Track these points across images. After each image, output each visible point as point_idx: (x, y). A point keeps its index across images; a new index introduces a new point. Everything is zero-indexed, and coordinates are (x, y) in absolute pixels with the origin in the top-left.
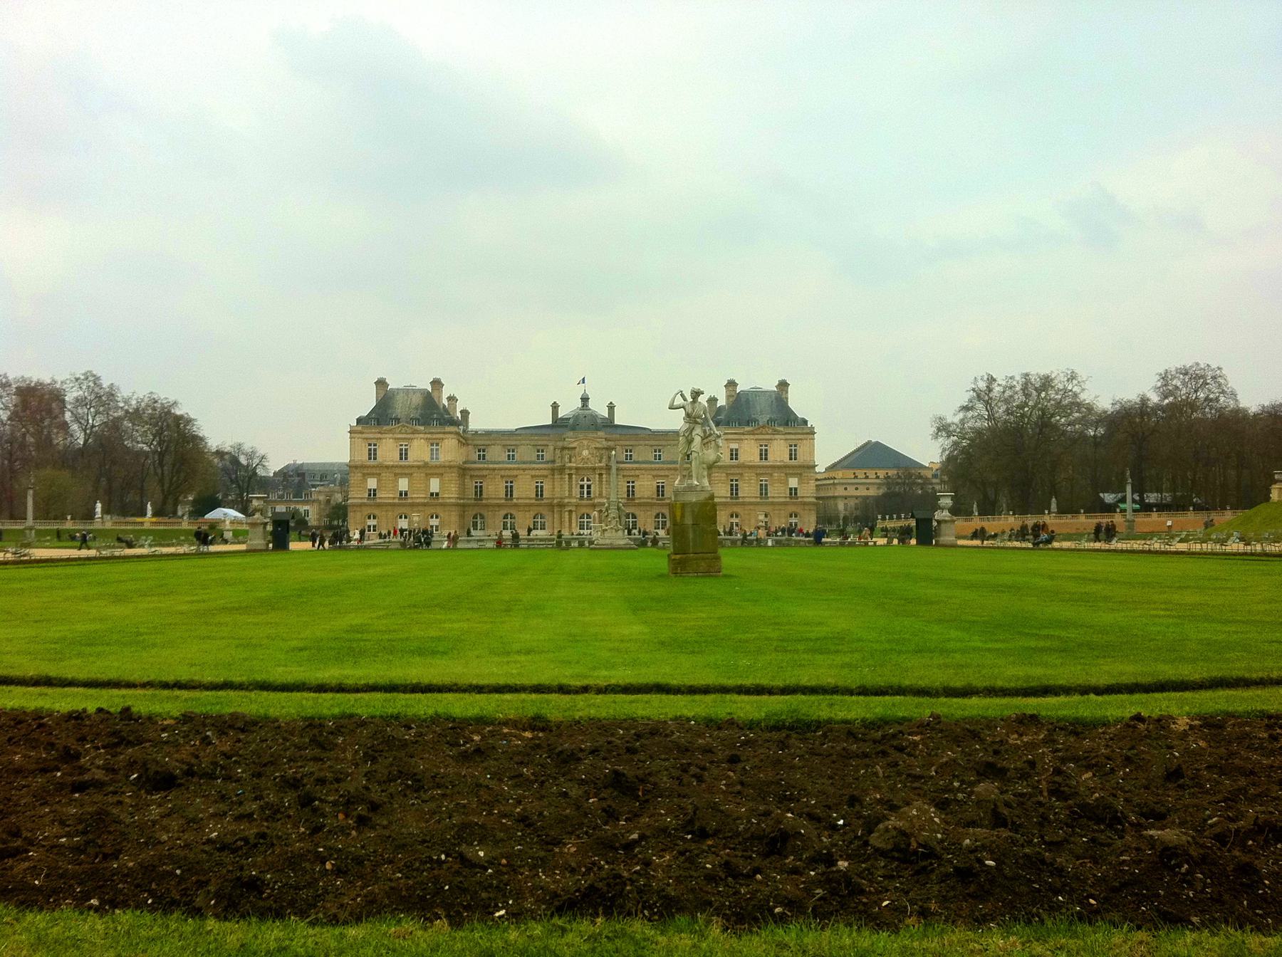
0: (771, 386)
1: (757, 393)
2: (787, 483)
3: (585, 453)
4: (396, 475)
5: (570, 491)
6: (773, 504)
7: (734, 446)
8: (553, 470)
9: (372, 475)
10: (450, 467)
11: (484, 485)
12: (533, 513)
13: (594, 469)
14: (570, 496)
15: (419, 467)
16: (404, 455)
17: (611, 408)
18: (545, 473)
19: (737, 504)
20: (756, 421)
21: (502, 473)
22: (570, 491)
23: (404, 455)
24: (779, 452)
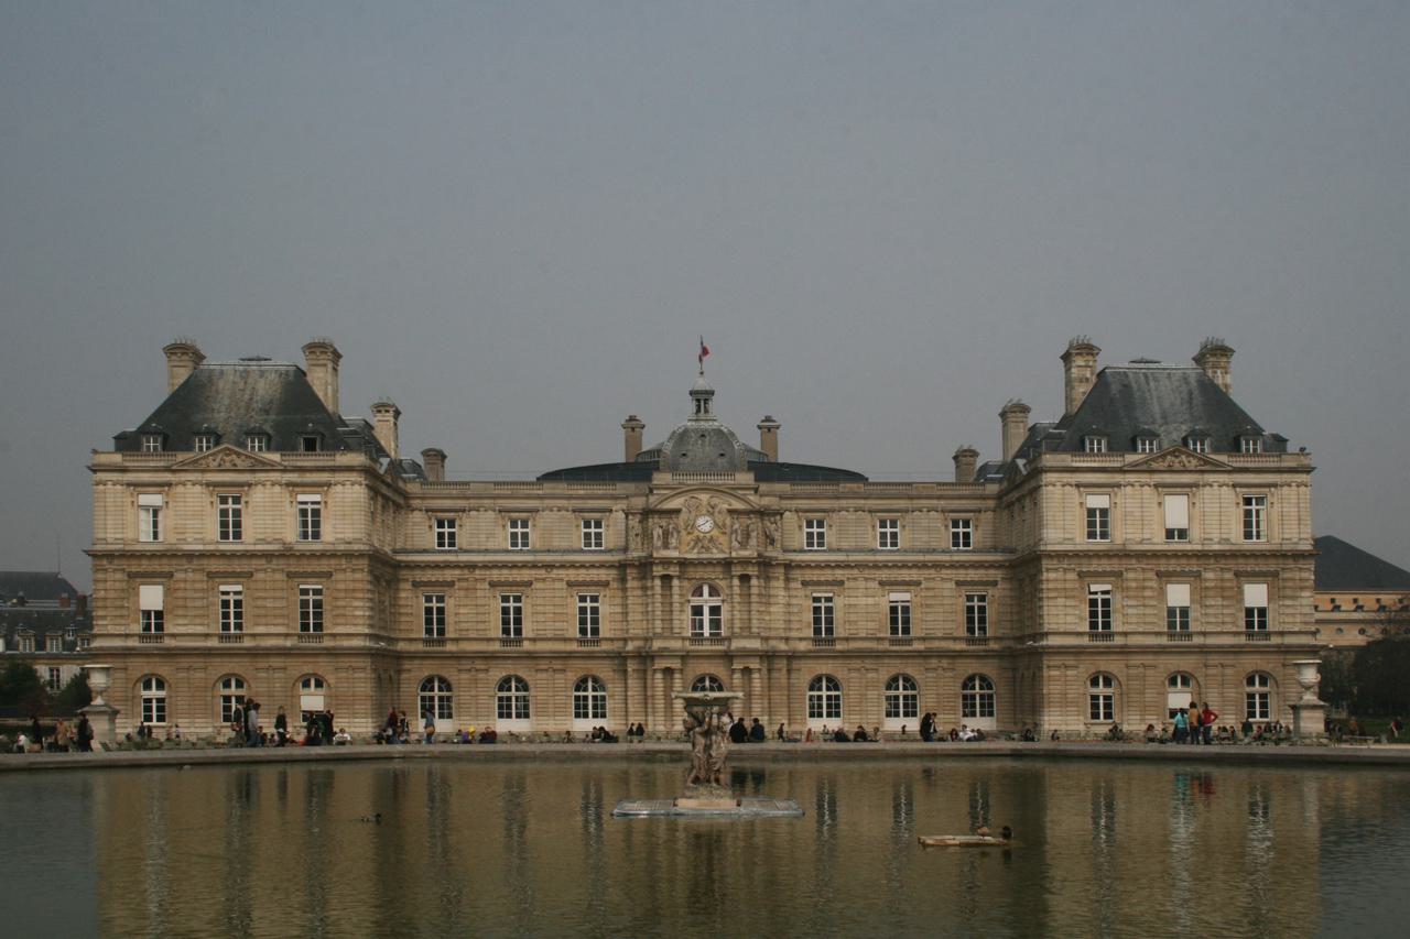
2: (1239, 595)
3: (705, 525)
4: (211, 575)
6: (1203, 650)
7: (1098, 501)
8: (622, 567)
9: (150, 577)
10: (349, 555)
11: (449, 604)
12: (573, 677)
13: (727, 564)
15: (268, 556)
16: (231, 526)
17: (768, 427)
18: (603, 575)
19: (1108, 651)
20: (1152, 435)
22: (668, 620)
23: (231, 526)
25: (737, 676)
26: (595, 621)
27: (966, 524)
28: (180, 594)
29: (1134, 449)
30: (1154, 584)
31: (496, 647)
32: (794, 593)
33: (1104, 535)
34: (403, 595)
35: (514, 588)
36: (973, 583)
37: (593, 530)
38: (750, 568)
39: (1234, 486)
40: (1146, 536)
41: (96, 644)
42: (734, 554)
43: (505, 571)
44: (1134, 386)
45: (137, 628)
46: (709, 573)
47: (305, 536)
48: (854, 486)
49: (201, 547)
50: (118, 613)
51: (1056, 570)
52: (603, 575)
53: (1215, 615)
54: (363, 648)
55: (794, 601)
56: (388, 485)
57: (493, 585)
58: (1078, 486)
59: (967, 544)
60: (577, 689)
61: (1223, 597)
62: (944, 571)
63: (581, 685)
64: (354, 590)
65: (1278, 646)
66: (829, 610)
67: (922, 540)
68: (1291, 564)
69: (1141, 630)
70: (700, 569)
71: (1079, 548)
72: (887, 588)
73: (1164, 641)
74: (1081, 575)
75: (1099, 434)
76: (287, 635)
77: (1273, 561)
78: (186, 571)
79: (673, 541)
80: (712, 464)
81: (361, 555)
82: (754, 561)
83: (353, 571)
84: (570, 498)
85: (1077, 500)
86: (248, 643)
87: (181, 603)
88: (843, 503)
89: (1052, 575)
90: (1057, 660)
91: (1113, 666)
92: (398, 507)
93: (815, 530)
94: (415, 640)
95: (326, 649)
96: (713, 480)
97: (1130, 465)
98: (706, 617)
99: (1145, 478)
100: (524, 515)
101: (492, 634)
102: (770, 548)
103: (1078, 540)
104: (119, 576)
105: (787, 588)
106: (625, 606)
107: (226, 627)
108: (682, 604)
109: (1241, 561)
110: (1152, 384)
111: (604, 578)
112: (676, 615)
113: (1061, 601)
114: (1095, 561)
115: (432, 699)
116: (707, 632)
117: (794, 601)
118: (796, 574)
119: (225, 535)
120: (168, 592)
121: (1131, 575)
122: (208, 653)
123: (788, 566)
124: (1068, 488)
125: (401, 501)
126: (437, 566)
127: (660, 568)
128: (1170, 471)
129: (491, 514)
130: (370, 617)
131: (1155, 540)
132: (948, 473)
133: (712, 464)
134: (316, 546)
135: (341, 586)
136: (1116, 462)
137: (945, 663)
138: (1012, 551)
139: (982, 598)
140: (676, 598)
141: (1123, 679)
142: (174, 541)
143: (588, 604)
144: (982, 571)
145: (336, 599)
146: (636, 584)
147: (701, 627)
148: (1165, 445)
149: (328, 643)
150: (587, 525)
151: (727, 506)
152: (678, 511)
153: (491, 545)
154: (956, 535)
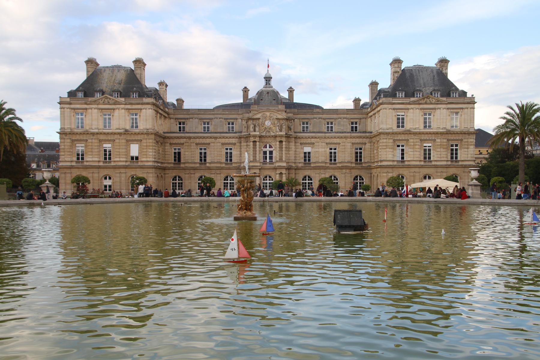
0: (431, 62)
1: (420, 69)
3: (268, 123)
4: (100, 141)
5: (255, 156)
6: (436, 167)
8: (240, 138)
10: (147, 134)
11: (182, 151)
12: (223, 176)
13: (276, 137)
15: (120, 134)
17: (291, 91)
18: (233, 141)
19: (403, 167)
21: (198, 141)
22: (255, 156)
23: (107, 123)
24: (442, 118)
25: (278, 175)
26: (231, 157)
27: (356, 123)
28: (90, 147)
29: (414, 97)
31: (198, 165)
32: (297, 147)
33: (403, 127)
34: (166, 148)
36: (357, 143)
37: (231, 126)
38: (283, 138)
39: (448, 109)
41: (61, 164)
42: (277, 134)
43: (201, 140)
44: (415, 74)
45: (75, 159)
46: (269, 140)
47: (132, 127)
48: (318, 110)
49: (97, 131)
50: (69, 153)
51: (386, 139)
52: (233, 141)
53: (440, 155)
54: (152, 165)
55: (297, 150)
56: (162, 110)
57: (197, 144)
59: (356, 130)
60: (225, 180)
61: (444, 148)
62: (348, 139)
63: (226, 179)
64: (149, 146)
65: (462, 165)
67: (341, 128)
68: (467, 136)
70: (266, 138)
71: (394, 131)
73: (422, 163)
74: (394, 141)
75: (402, 91)
76: (126, 161)
77: (461, 135)
78: (92, 139)
79: (257, 129)
80: (271, 102)
81: (152, 134)
83: (149, 139)
84: (223, 114)
85: (394, 114)
86: (112, 164)
87: (90, 150)
88: (315, 116)
89: (385, 141)
90: (385, 170)
92: (165, 117)
93: (305, 126)
94: (171, 163)
95: (139, 166)
96: (271, 108)
97: (412, 101)
98: (268, 155)
99: (417, 106)
100: (208, 120)
101: (196, 161)
102: (290, 131)
103: (394, 128)
104: (69, 141)
105: (295, 146)
106: (240, 151)
107: (105, 159)
108: (260, 151)
109: (450, 135)
110: (421, 73)
111: (234, 142)
112: (257, 155)
113: (388, 150)
114: (399, 136)
115: (176, 183)
116: (268, 160)
117: (297, 150)
118: (299, 141)
119: (105, 126)
120: (86, 146)
121: (412, 140)
122: (99, 167)
123: (296, 138)
125: (166, 115)
126: (178, 138)
127: (252, 138)
128: (426, 103)
129: (197, 120)
130: (155, 155)
132: (350, 105)
133: (271, 102)
134: (137, 131)
135: (145, 144)
136: (407, 100)
137: (348, 171)
138: (371, 132)
139: (361, 149)
140: (258, 149)
141: (408, 177)
142: (88, 128)
143: (229, 151)
144: (361, 139)
145: (143, 149)
146: (245, 144)
147: (266, 159)
148: (425, 94)
149: (140, 164)
150: (229, 124)
151: (275, 117)
152: (259, 119)
153: (197, 131)
154: (352, 127)
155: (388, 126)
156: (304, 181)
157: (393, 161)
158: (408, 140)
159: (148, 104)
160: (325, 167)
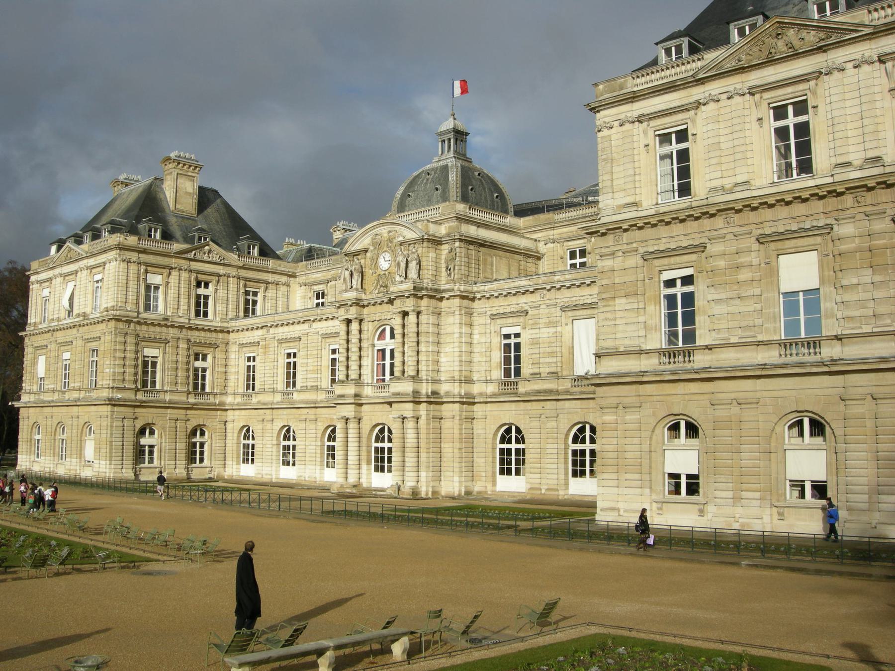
3: (384, 263)
6: (835, 369)
14: (347, 376)
30: (754, 258)
35: (292, 344)
40: (740, 179)
43: (286, 329)
53: (861, 304)
57: (281, 341)
58: (640, 120)
66: (518, 346)
69: (734, 340)
72: (570, 314)
74: (647, 257)
79: (354, 282)
82: (406, 294)
91: (691, 401)
124: (628, 126)
128: (771, 61)
131: (757, 183)
147: (384, 375)
152: (366, 251)
155: (622, 199)
156: (506, 446)
157: (641, 352)
158: (702, 248)
159: (110, 249)
160: (557, 392)
